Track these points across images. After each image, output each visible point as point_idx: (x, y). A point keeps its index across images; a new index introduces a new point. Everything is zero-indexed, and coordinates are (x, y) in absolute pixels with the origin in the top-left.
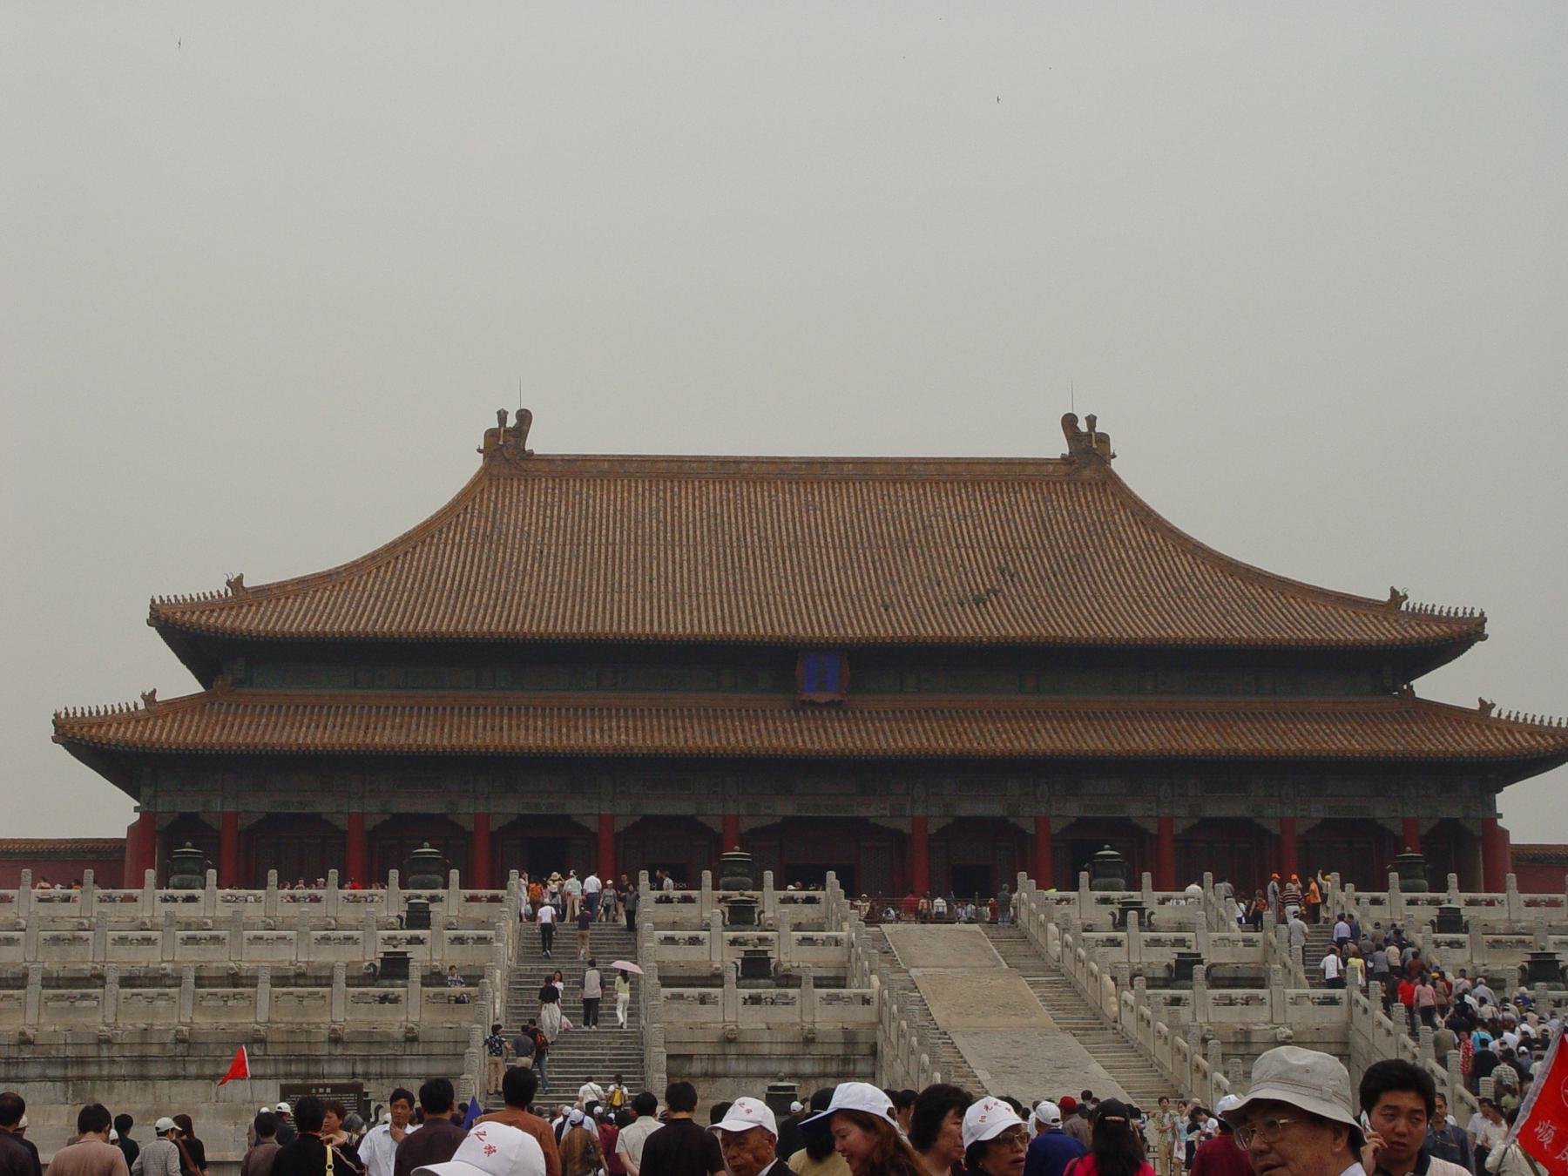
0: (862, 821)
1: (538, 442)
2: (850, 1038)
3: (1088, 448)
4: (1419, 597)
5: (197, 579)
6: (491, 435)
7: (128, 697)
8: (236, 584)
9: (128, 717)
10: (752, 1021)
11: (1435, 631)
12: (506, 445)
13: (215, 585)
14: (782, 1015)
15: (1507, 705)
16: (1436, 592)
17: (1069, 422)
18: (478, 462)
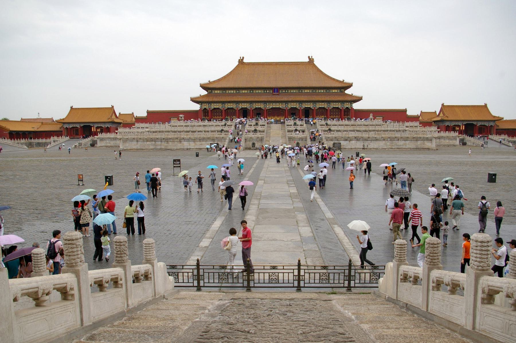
1: (245, 61)
2: (261, 137)
3: (311, 60)
4: (346, 81)
5: (205, 81)
6: (239, 60)
7: (198, 95)
8: (209, 81)
9: (198, 98)
10: (253, 136)
11: (347, 85)
12: (241, 61)
13: (207, 82)
14: (256, 135)
15: (355, 94)
16: (347, 80)
17: (309, 57)
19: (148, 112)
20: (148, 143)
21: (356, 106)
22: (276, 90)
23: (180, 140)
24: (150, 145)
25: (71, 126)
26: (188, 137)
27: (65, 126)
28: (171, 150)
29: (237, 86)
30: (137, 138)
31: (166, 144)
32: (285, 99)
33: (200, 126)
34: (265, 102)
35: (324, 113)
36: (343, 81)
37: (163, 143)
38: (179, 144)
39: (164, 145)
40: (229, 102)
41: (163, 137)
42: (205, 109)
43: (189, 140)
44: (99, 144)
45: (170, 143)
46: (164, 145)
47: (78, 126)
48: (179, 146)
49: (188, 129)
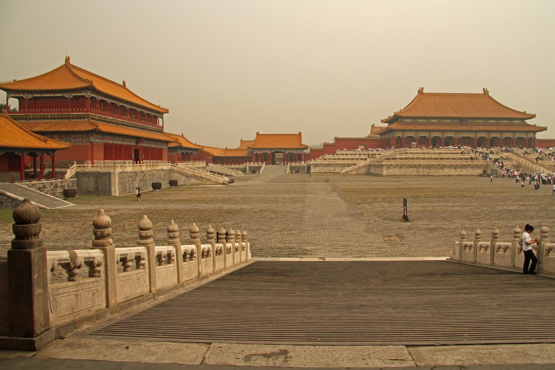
0: (469, 137)
1: (424, 91)
3: (486, 92)
6: (419, 91)
12: (420, 92)
15: (538, 125)
17: (484, 89)
18: (417, 94)
19: (336, 139)
20: (411, 169)
21: (539, 136)
22: (461, 120)
23: (443, 167)
24: (414, 172)
25: (261, 152)
26: (450, 163)
27: (255, 152)
28: (433, 176)
29: (428, 115)
30: (401, 164)
31: (428, 171)
32: (474, 128)
33: (436, 153)
34: (456, 131)
35: (508, 143)
36: (525, 112)
37: (425, 170)
38: (441, 171)
39: (426, 172)
40: (423, 131)
41: (425, 163)
42: (399, 137)
43: (450, 167)
44: (313, 170)
45: (432, 170)
46: (426, 172)
47: (269, 152)
48: (441, 172)
49: (435, 156)
